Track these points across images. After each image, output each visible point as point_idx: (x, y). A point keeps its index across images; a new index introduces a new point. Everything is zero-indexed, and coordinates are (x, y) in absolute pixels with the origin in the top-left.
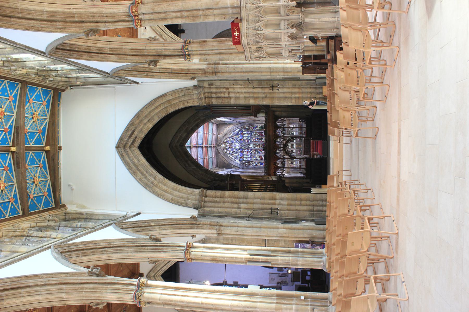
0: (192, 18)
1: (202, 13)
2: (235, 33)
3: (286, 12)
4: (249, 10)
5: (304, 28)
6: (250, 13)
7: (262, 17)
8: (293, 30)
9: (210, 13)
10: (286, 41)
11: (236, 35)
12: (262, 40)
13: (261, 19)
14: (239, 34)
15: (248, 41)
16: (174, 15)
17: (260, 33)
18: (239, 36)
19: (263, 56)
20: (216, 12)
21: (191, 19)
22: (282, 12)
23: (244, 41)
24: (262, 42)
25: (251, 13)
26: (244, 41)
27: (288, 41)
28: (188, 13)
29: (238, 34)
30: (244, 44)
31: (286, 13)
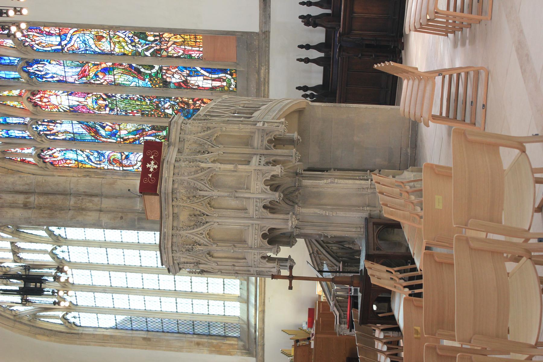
0: (48, 211)
1: (75, 203)
2: (150, 163)
3: (265, 142)
4: (187, 132)
5: (299, 201)
6: (189, 137)
7: (213, 147)
8: (276, 196)
9: (91, 204)
10: (260, 191)
11: (151, 170)
12: (207, 185)
13: (211, 150)
14: (158, 168)
15: (176, 186)
16: (9, 198)
17: (204, 196)
18: (157, 173)
19: (202, 241)
20: (107, 203)
21: (45, 212)
22: (256, 142)
23: (166, 179)
24: (206, 189)
25: (192, 137)
26: (166, 179)
27: (263, 192)
28: (42, 200)
29: (156, 167)
30: (165, 186)
31: (264, 144)
